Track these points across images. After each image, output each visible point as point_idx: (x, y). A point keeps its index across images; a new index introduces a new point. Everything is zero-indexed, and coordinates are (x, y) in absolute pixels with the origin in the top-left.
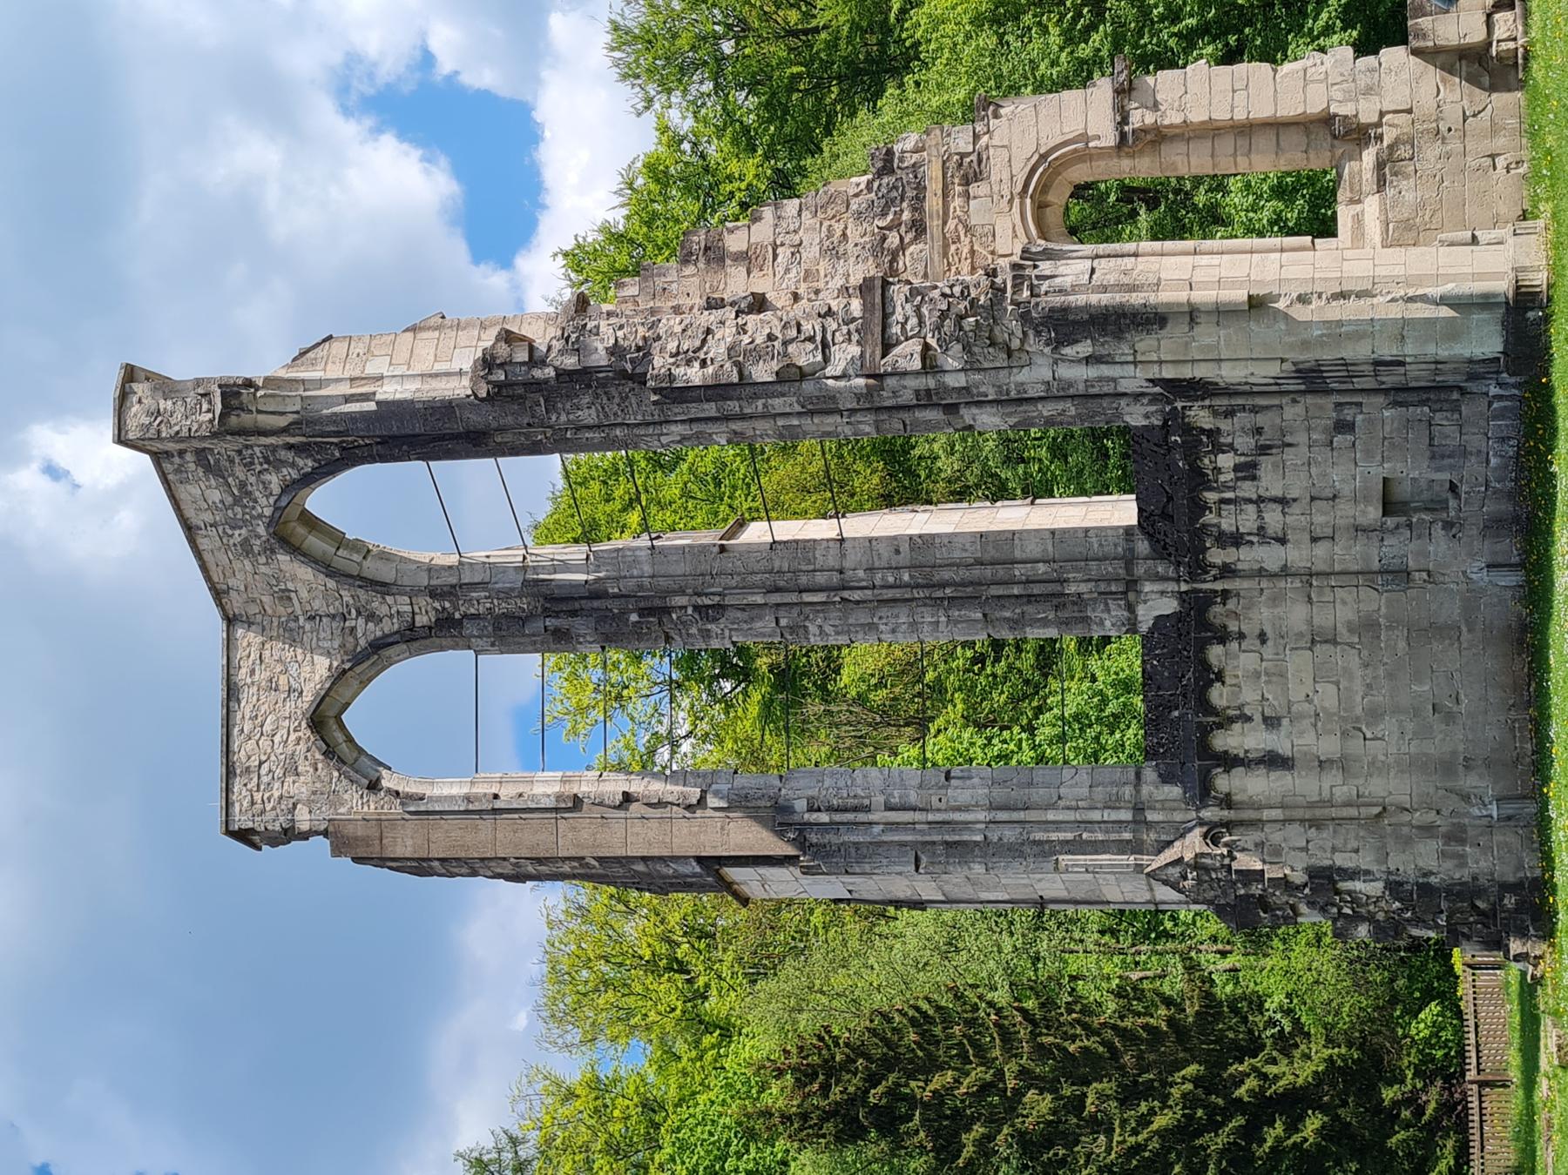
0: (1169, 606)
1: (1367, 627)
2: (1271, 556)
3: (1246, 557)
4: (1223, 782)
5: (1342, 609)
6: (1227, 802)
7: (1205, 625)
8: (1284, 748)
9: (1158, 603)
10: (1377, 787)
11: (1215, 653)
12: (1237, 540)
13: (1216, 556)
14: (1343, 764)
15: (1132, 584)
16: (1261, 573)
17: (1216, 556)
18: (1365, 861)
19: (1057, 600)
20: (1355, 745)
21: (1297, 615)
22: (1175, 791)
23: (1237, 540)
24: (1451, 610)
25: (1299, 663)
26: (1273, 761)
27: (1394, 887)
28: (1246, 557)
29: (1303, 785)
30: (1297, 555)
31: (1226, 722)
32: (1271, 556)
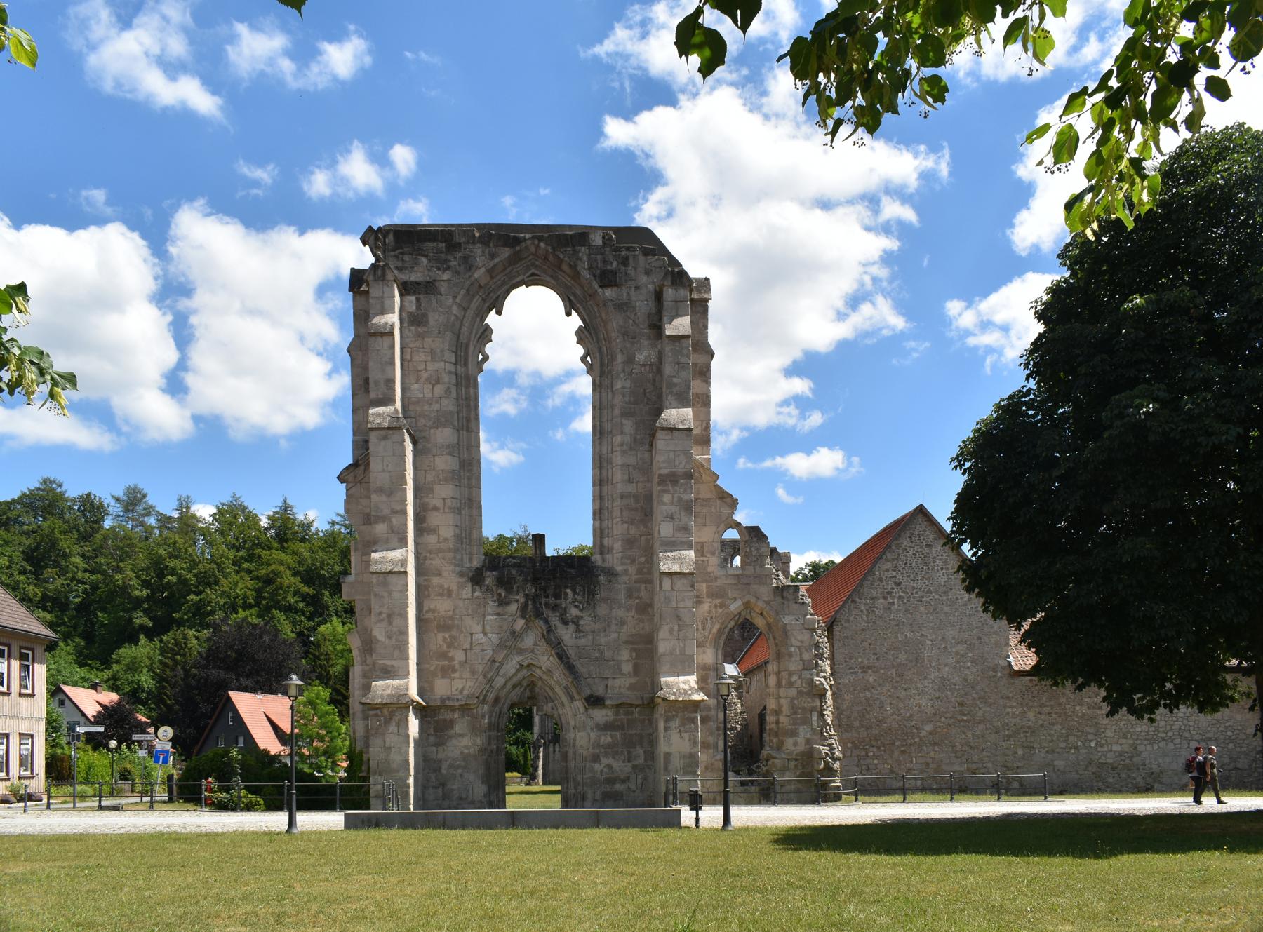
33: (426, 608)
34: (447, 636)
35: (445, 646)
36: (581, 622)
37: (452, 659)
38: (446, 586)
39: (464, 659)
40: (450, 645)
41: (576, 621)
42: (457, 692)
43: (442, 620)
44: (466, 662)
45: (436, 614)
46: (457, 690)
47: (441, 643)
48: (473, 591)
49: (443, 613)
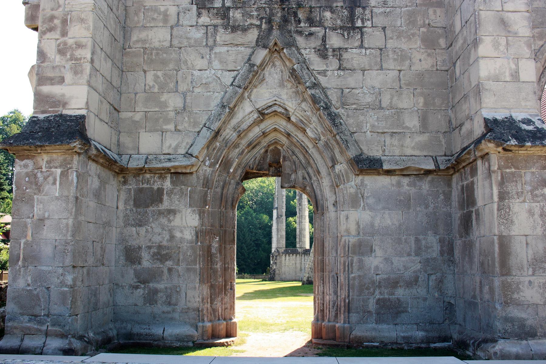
0: (299, 251)
1: (296, 268)
2: (303, 260)
3: (303, 258)
4: (284, 255)
5: (298, 265)
6: (282, 255)
7: (297, 254)
8: (286, 260)
9: (299, 250)
10: (283, 268)
11: (295, 255)
12: (304, 257)
13: (303, 255)
14: (285, 265)
15: (301, 248)
16: (301, 259)
17: (303, 255)
18: (277, 267)
19: (300, 241)
20: (287, 266)
21: (298, 262)
22: (283, 251)
23: (304, 257)
24: (298, 274)
25: (294, 262)
26: (285, 259)
27: (275, 269)
28: (303, 258)
29: (283, 262)
30: (303, 262)
31: (289, 256)
32: (303, 260)
33: (134, 38)
34: (160, 74)
35: (157, 87)
36: (345, 56)
37: (165, 105)
38: (162, 9)
39: (181, 105)
40: (163, 87)
41: (338, 52)
42: (170, 151)
43: (154, 52)
44: (184, 108)
45: (147, 46)
46: (170, 146)
47: (151, 84)
48: (199, 15)
49: (157, 44)
